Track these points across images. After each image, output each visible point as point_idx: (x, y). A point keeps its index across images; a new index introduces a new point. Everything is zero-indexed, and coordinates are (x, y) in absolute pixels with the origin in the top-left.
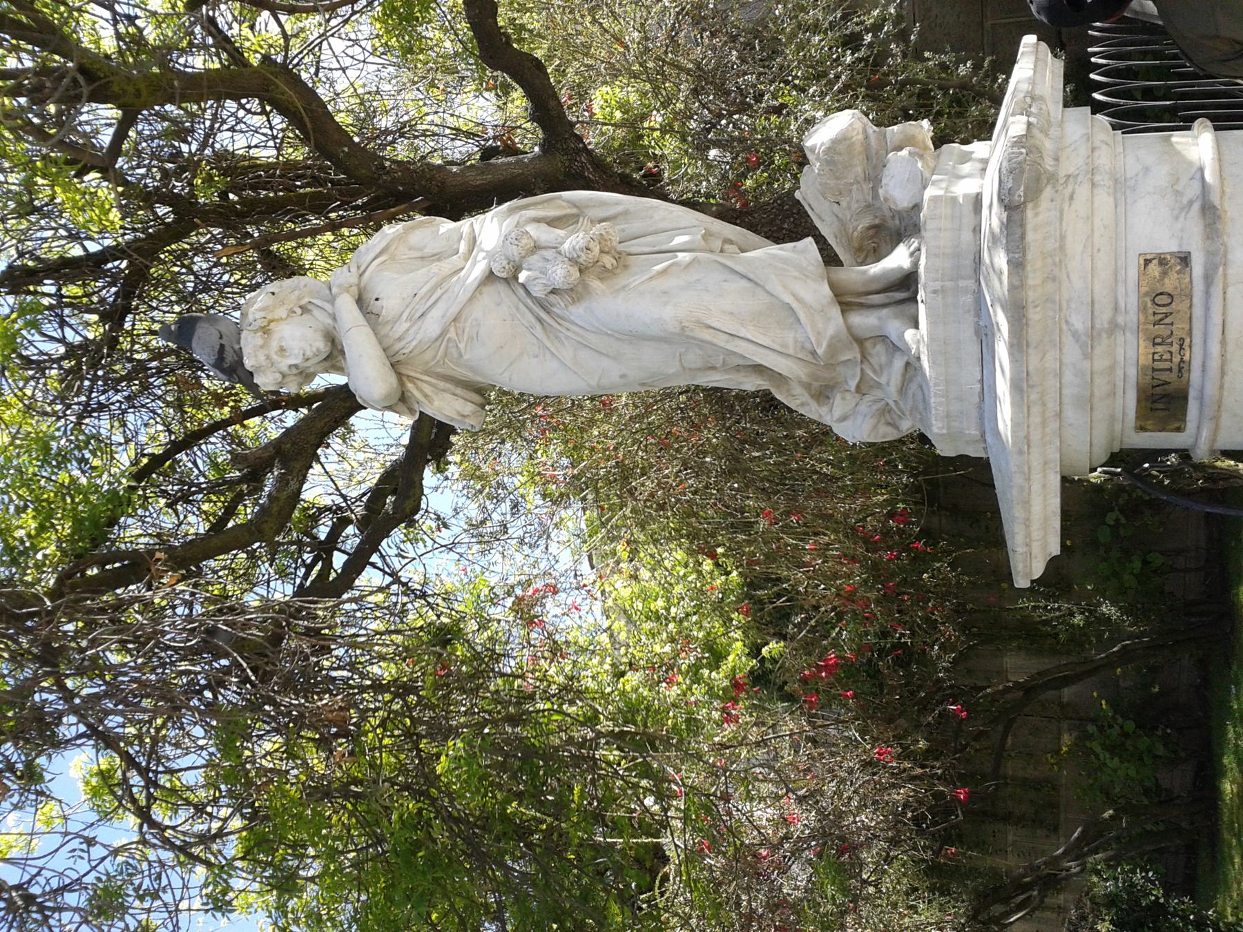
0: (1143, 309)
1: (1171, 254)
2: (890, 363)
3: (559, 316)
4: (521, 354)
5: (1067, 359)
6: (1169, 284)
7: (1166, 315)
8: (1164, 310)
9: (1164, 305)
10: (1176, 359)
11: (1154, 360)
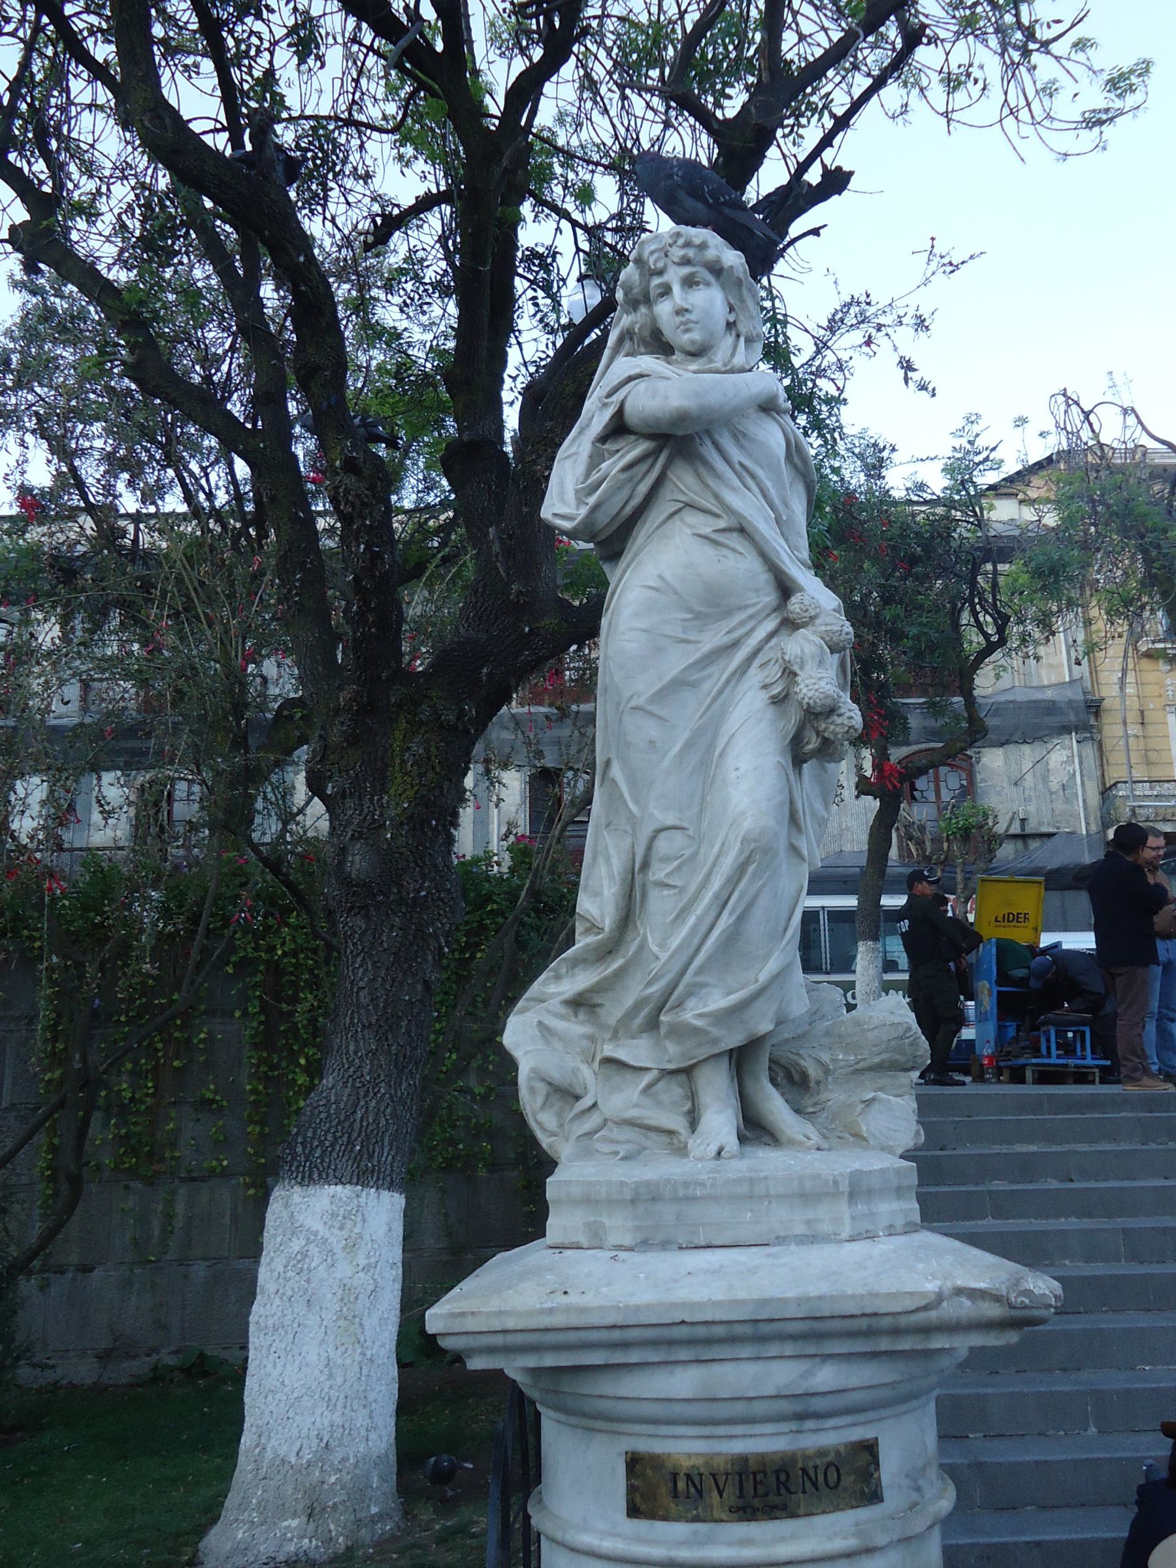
0: (821, 1453)
1: (879, 1478)
2: (659, 1104)
3: (744, 672)
4: (690, 610)
5: (774, 1366)
6: (848, 1480)
7: (815, 1485)
8: (821, 1478)
9: (825, 1474)
10: (757, 1503)
11: (754, 1474)
